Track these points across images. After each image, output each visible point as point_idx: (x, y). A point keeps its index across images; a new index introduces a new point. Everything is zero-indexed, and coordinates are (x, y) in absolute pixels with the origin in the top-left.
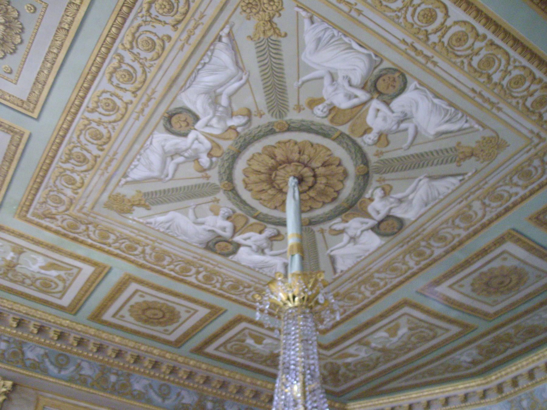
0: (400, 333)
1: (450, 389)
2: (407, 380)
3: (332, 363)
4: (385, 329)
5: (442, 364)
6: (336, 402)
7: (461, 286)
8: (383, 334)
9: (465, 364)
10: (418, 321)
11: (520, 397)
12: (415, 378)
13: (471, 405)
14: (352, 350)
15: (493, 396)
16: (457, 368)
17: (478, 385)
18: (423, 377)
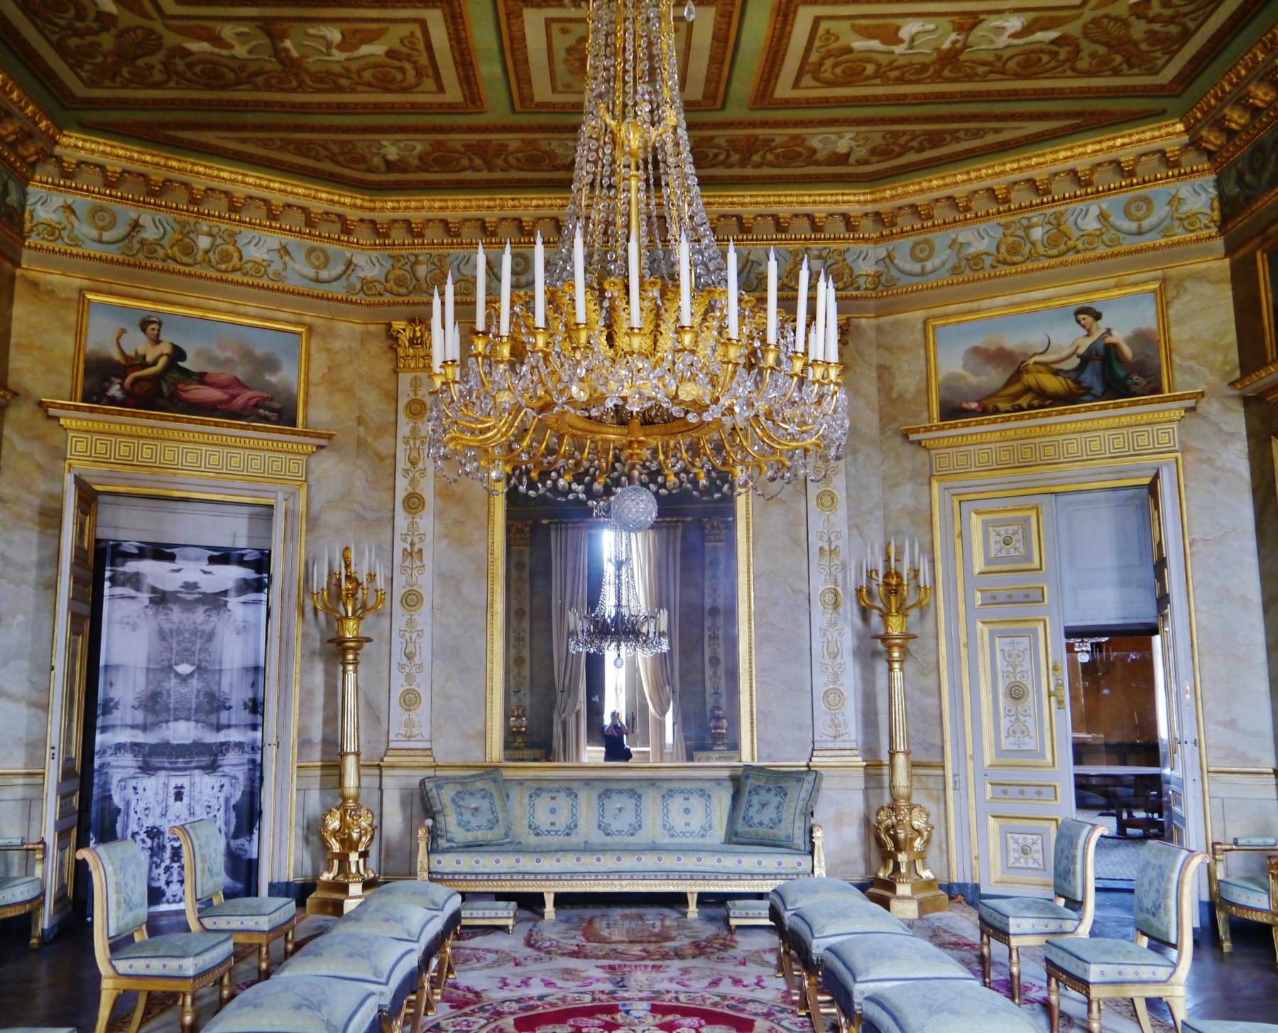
0: (365, 49)
1: (301, 191)
2: (244, 141)
3: (151, 32)
4: (346, 26)
5: (343, 143)
6: (48, 117)
7: (565, 31)
8: (334, 35)
9: (376, 161)
10: (421, 46)
11: (416, 256)
12: (265, 144)
13: (320, 236)
14: (228, 31)
15: (363, 235)
16: (357, 160)
17: (354, 206)
18: (281, 149)
